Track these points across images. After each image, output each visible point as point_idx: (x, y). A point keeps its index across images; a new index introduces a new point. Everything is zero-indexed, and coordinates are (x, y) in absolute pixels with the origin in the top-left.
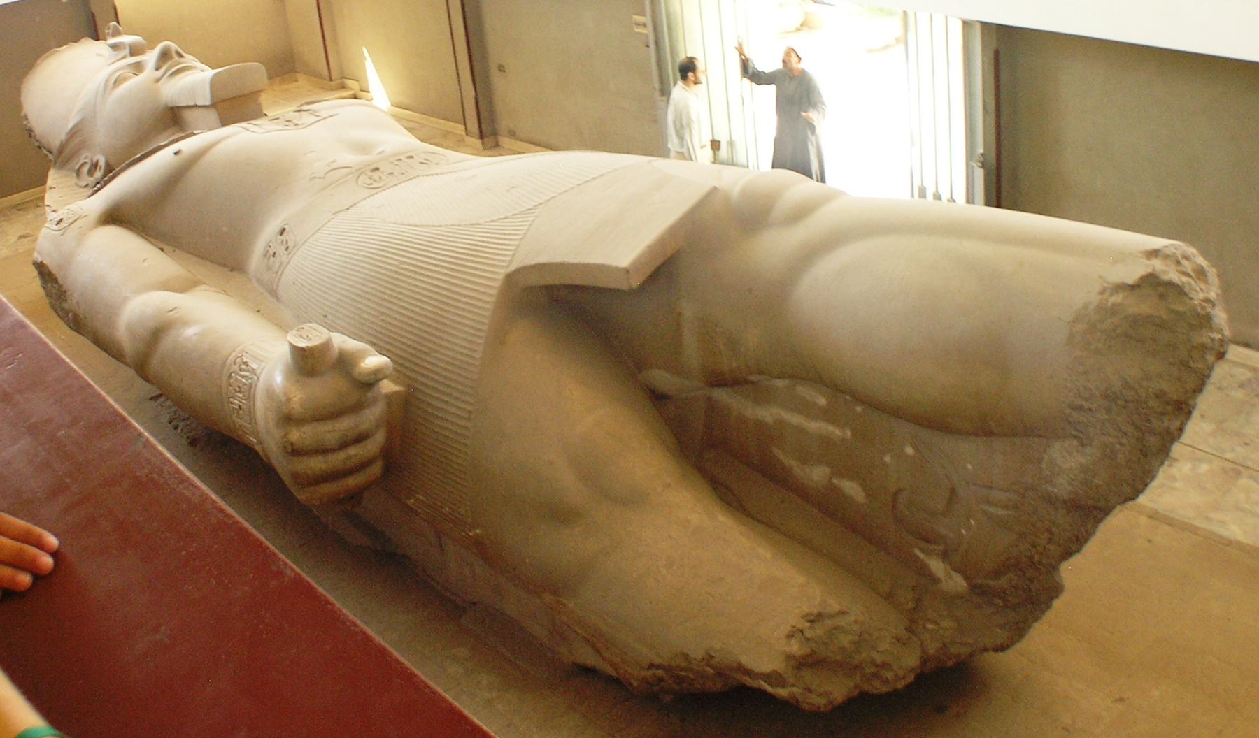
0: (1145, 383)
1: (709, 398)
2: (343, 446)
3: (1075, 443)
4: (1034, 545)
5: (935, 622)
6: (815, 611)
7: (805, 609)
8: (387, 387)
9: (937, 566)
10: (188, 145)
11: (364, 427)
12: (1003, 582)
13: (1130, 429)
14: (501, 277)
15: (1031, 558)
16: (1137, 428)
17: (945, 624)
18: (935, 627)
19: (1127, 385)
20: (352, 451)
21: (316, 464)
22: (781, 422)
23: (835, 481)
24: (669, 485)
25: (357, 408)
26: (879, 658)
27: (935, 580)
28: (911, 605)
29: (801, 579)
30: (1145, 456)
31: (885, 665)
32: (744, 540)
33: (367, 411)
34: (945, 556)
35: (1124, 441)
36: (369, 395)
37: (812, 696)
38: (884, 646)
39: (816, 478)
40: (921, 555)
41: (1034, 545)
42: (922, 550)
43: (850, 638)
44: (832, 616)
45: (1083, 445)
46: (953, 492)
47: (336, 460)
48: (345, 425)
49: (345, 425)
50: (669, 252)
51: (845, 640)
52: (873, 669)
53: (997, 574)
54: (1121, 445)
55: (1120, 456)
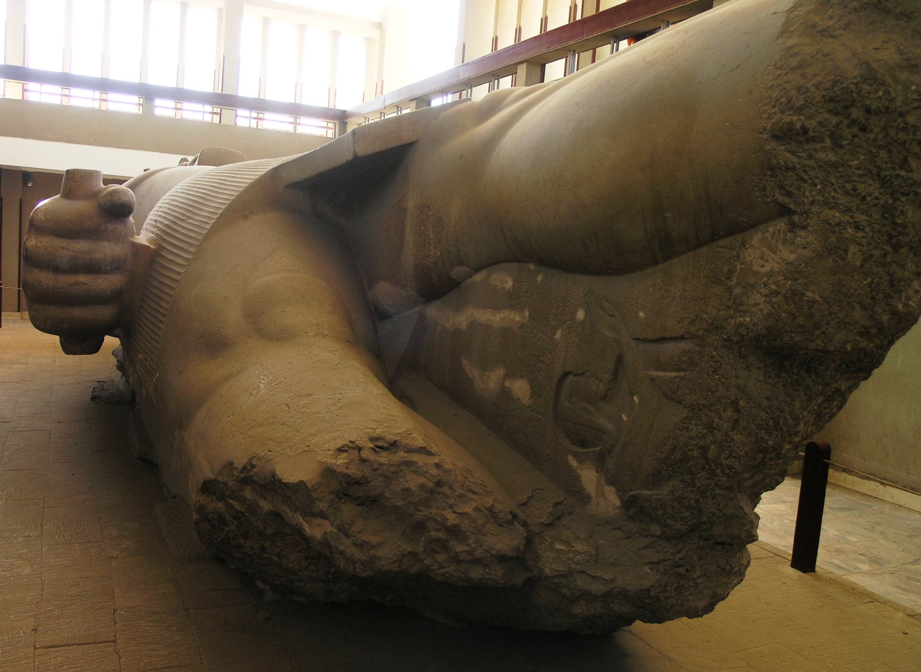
0: (904, 76)
1: (422, 317)
3: (782, 224)
4: (710, 428)
6: (391, 437)
9: (589, 477)
12: (663, 491)
13: (871, 188)
15: (704, 450)
16: (884, 182)
17: (578, 546)
20: (82, 278)
21: (46, 279)
22: (473, 325)
23: (507, 384)
26: (451, 518)
27: (585, 498)
30: (896, 247)
31: (455, 532)
33: (106, 244)
34: (600, 461)
35: (862, 218)
36: (110, 226)
37: (348, 542)
38: (468, 509)
39: (491, 386)
40: (573, 462)
41: (710, 428)
42: (575, 455)
43: (422, 480)
44: (410, 451)
45: (793, 226)
46: (620, 359)
47: (66, 281)
50: (406, 138)
51: (413, 482)
52: (441, 535)
53: (656, 479)
54: (857, 227)
55: (853, 248)
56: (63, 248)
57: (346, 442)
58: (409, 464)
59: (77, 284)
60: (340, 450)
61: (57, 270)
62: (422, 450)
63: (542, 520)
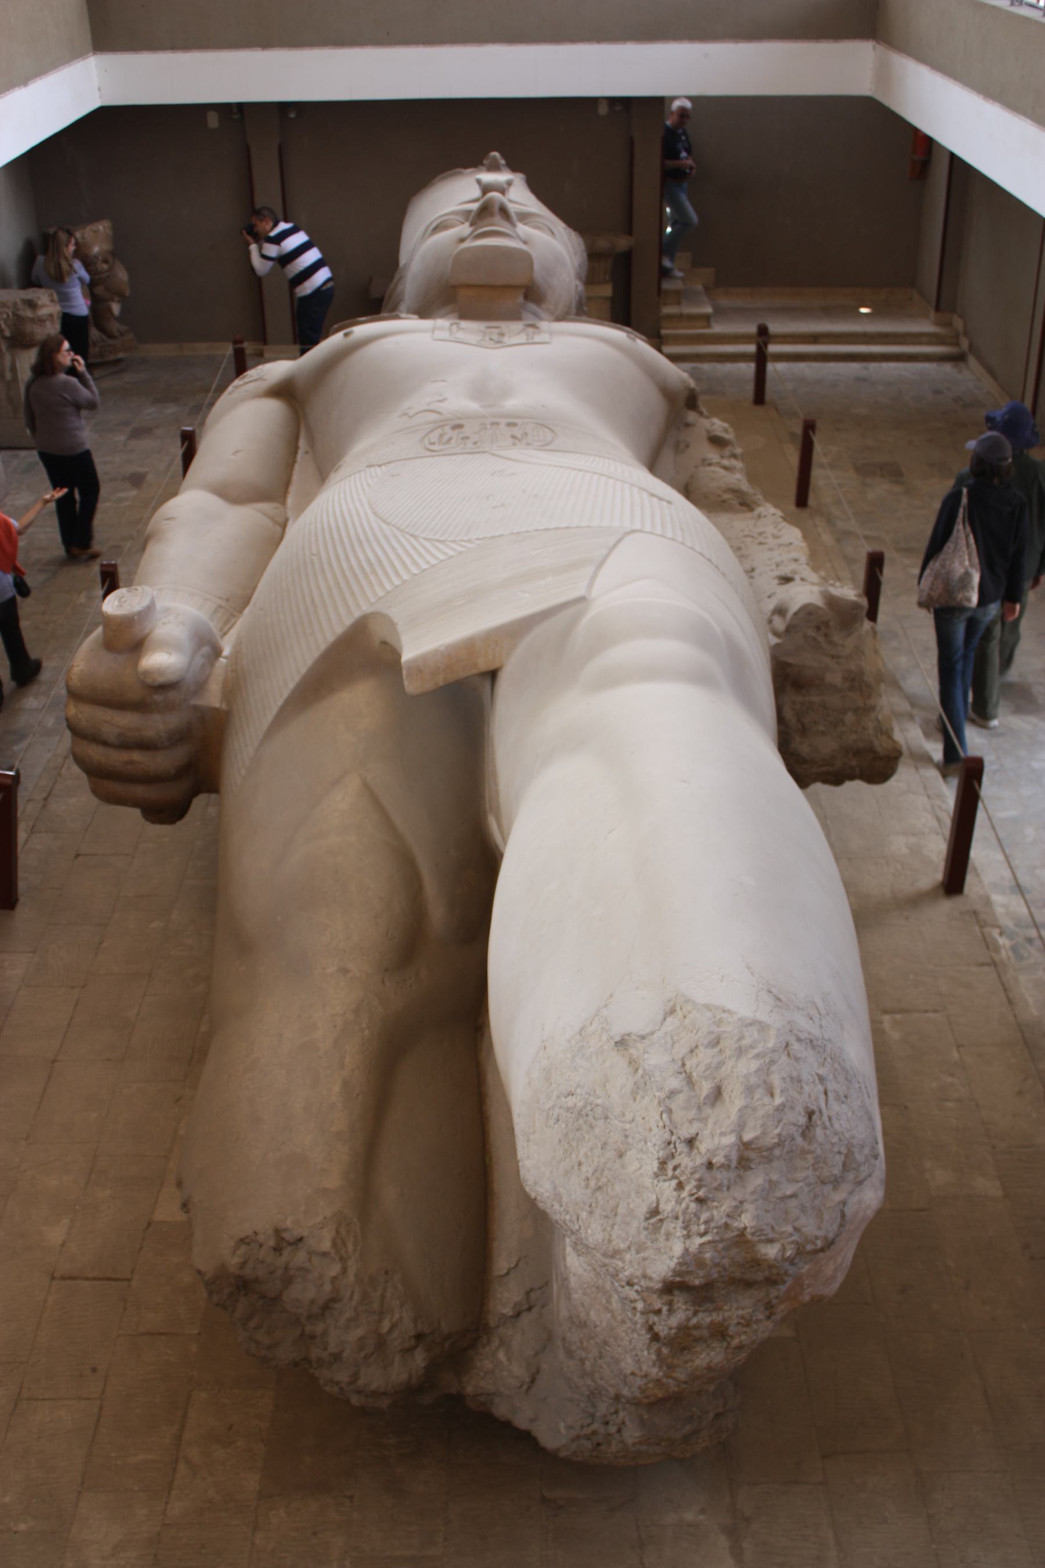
2: (126, 744)
5: (509, 1359)
6: (298, 1232)
7: (289, 1223)
8: (213, 698)
10: (362, 330)
11: (149, 733)
14: (357, 614)
18: (505, 1363)
19: (558, 1197)
20: (136, 756)
21: (96, 753)
24: (345, 971)
25: (141, 706)
28: (508, 1311)
29: (334, 1181)
32: (337, 1088)
33: (156, 717)
44: (311, 1253)
48: (126, 721)
49: (126, 721)
56: (106, 722)
57: (250, 1232)
58: (308, 1271)
59: (131, 762)
60: (242, 1241)
61: (105, 743)
62: (325, 1254)
63: (505, 1311)
